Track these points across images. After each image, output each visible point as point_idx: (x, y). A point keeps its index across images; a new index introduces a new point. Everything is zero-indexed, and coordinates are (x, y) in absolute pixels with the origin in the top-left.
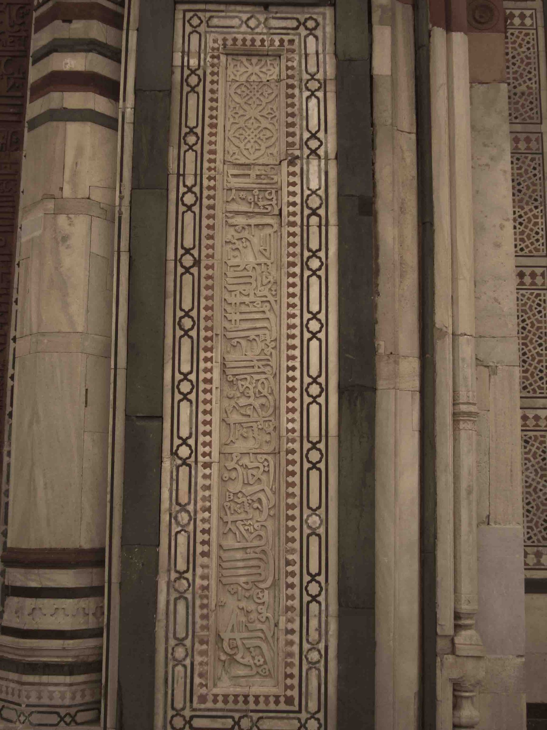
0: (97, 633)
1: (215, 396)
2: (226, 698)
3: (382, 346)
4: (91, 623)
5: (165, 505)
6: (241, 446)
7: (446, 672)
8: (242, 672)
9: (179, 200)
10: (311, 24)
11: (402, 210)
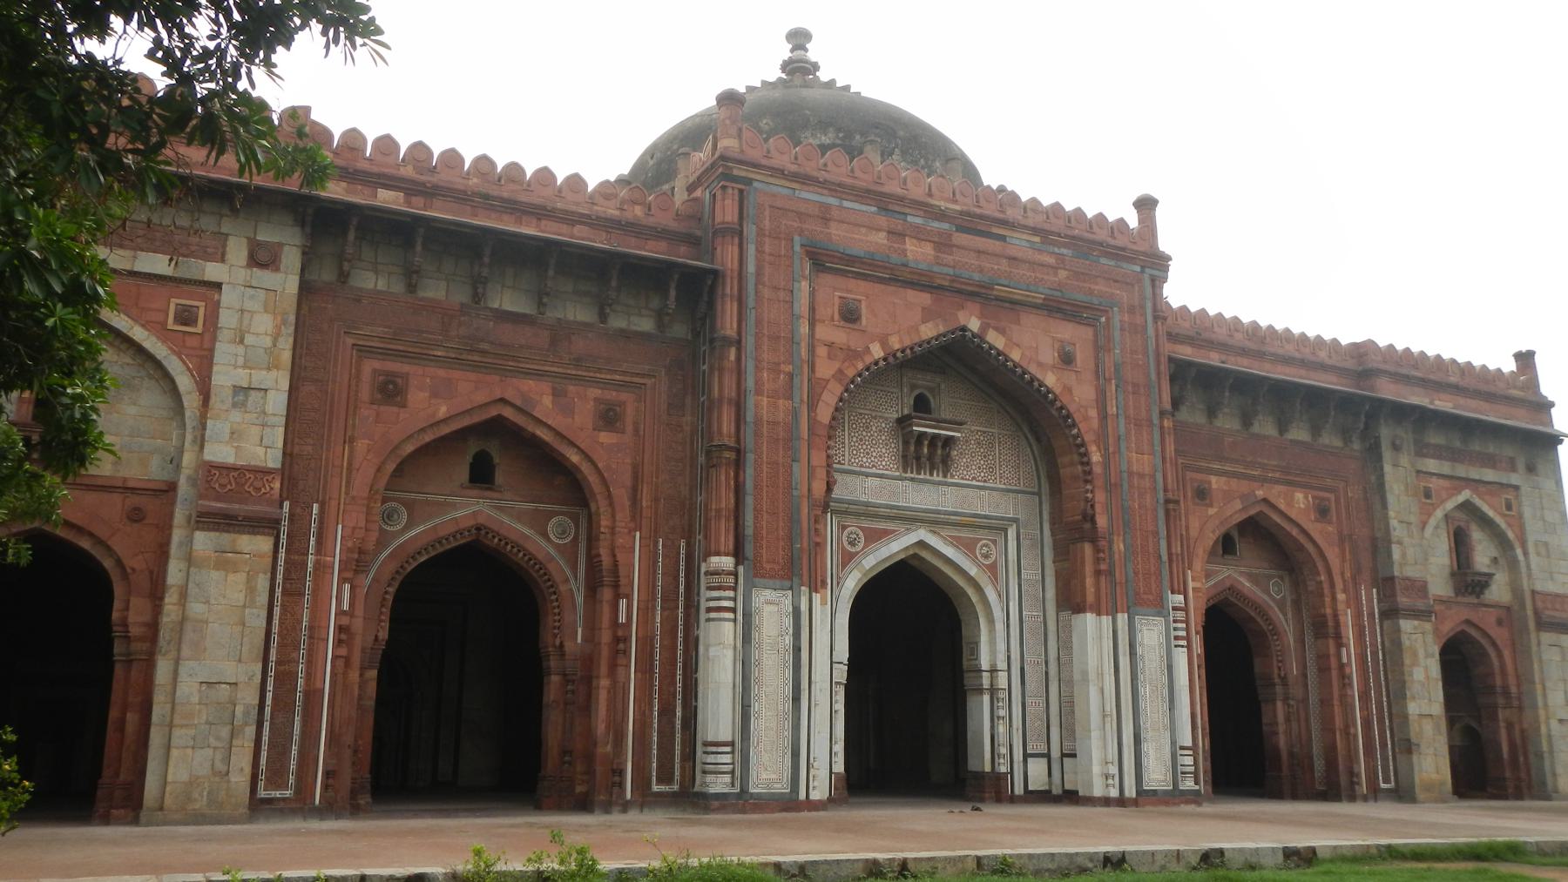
7: (812, 772)
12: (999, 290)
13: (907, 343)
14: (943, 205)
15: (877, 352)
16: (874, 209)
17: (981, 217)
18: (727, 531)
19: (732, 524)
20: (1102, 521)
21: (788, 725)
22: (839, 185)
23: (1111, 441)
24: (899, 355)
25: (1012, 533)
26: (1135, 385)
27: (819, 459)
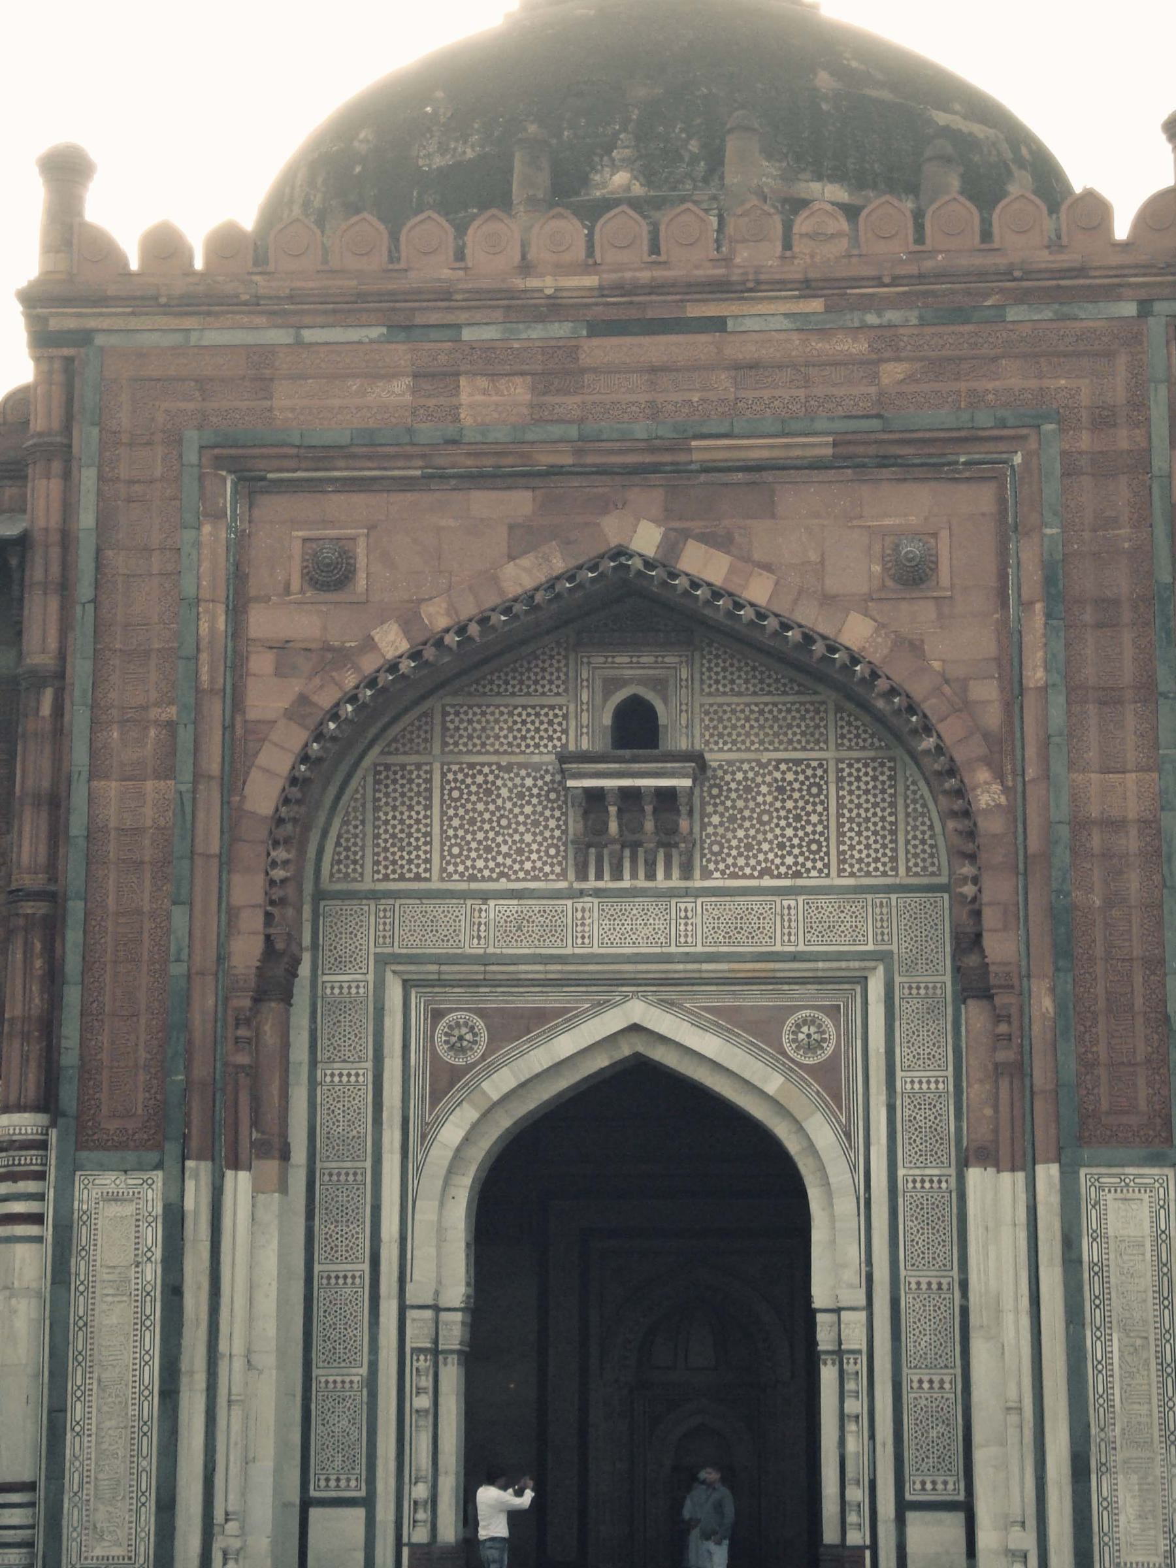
0: (32, 1527)
1: (94, 1398)
2: (98, 1558)
3: (184, 1366)
4: (30, 1521)
5: (68, 1457)
6: (108, 1424)
7: (218, 1544)
8: (106, 1544)
9: (76, 1288)
10: (150, 1181)
11: (199, 1288)
12: (702, 450)
13: (468, 609)
14: (548, 284)
15: (392, 642)
16: (375, 332)
17: (654, 288)
18: (25, 1059)
19: (35, 1050)
20: (1000, 947)
21: (151, 1445)
22: (291, 298)
23: (1031, 752)
24: (452, 639)
25: (876, 987)
26: (1107, 605)
27: (248, 890)
